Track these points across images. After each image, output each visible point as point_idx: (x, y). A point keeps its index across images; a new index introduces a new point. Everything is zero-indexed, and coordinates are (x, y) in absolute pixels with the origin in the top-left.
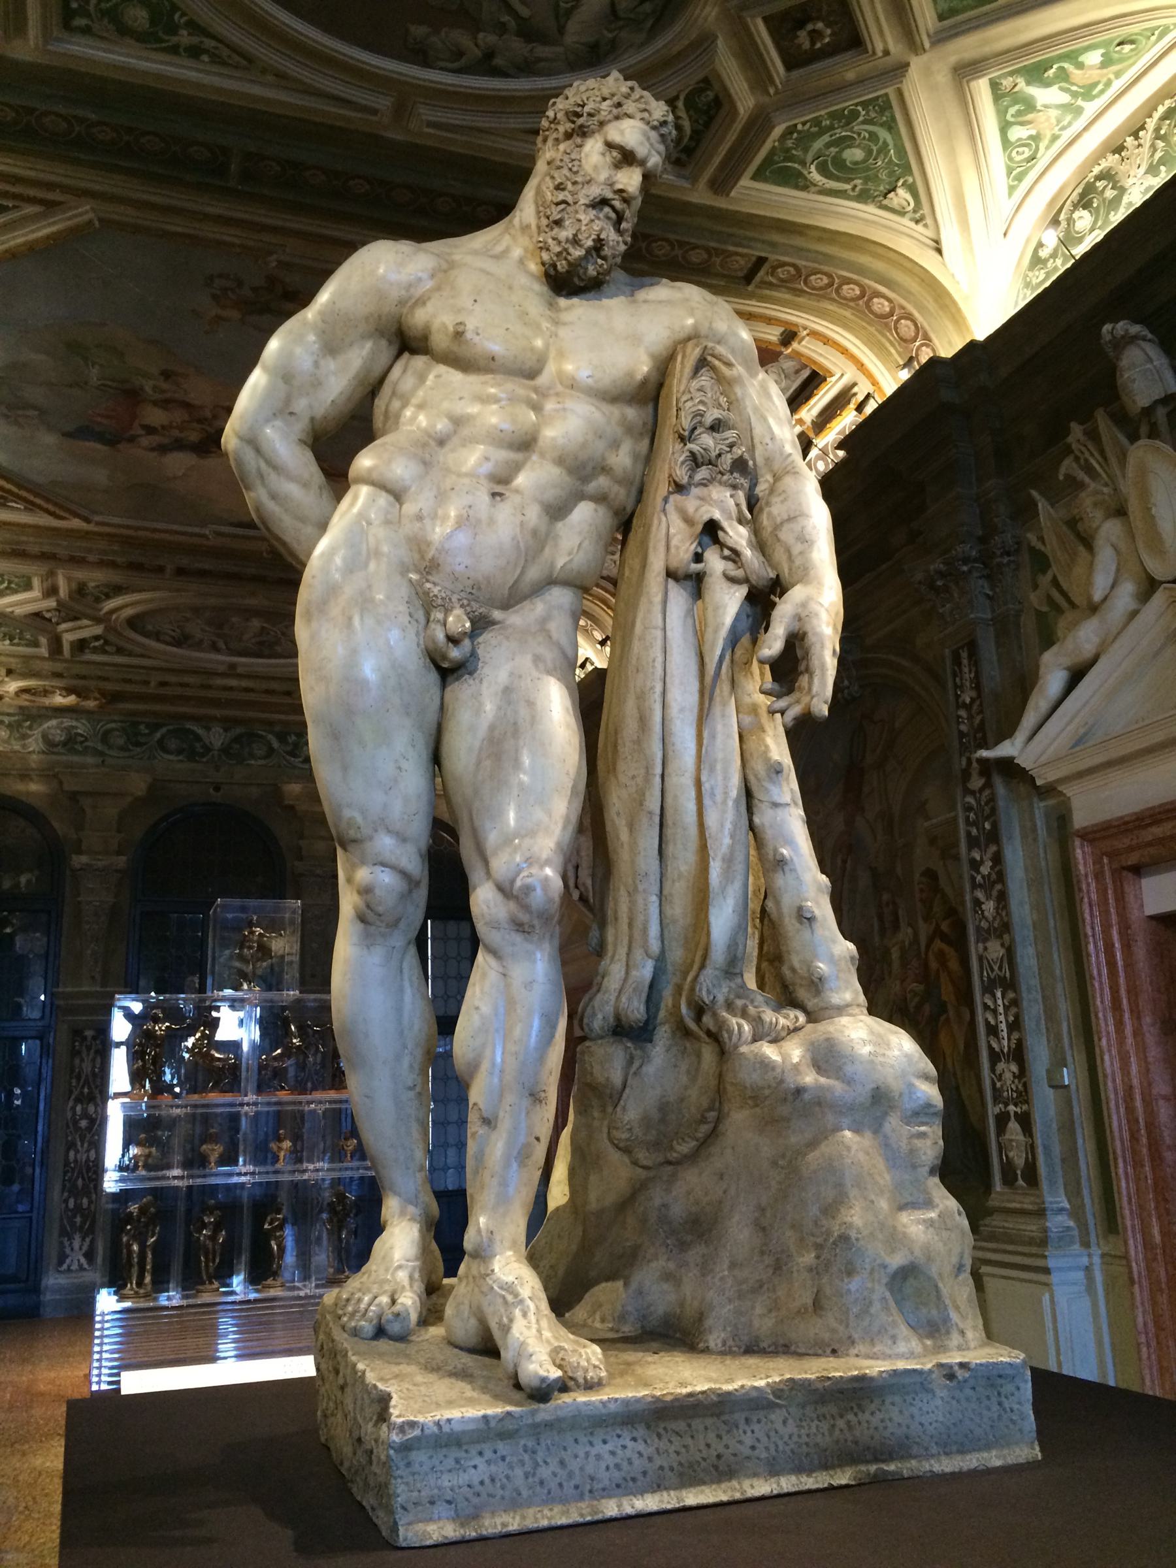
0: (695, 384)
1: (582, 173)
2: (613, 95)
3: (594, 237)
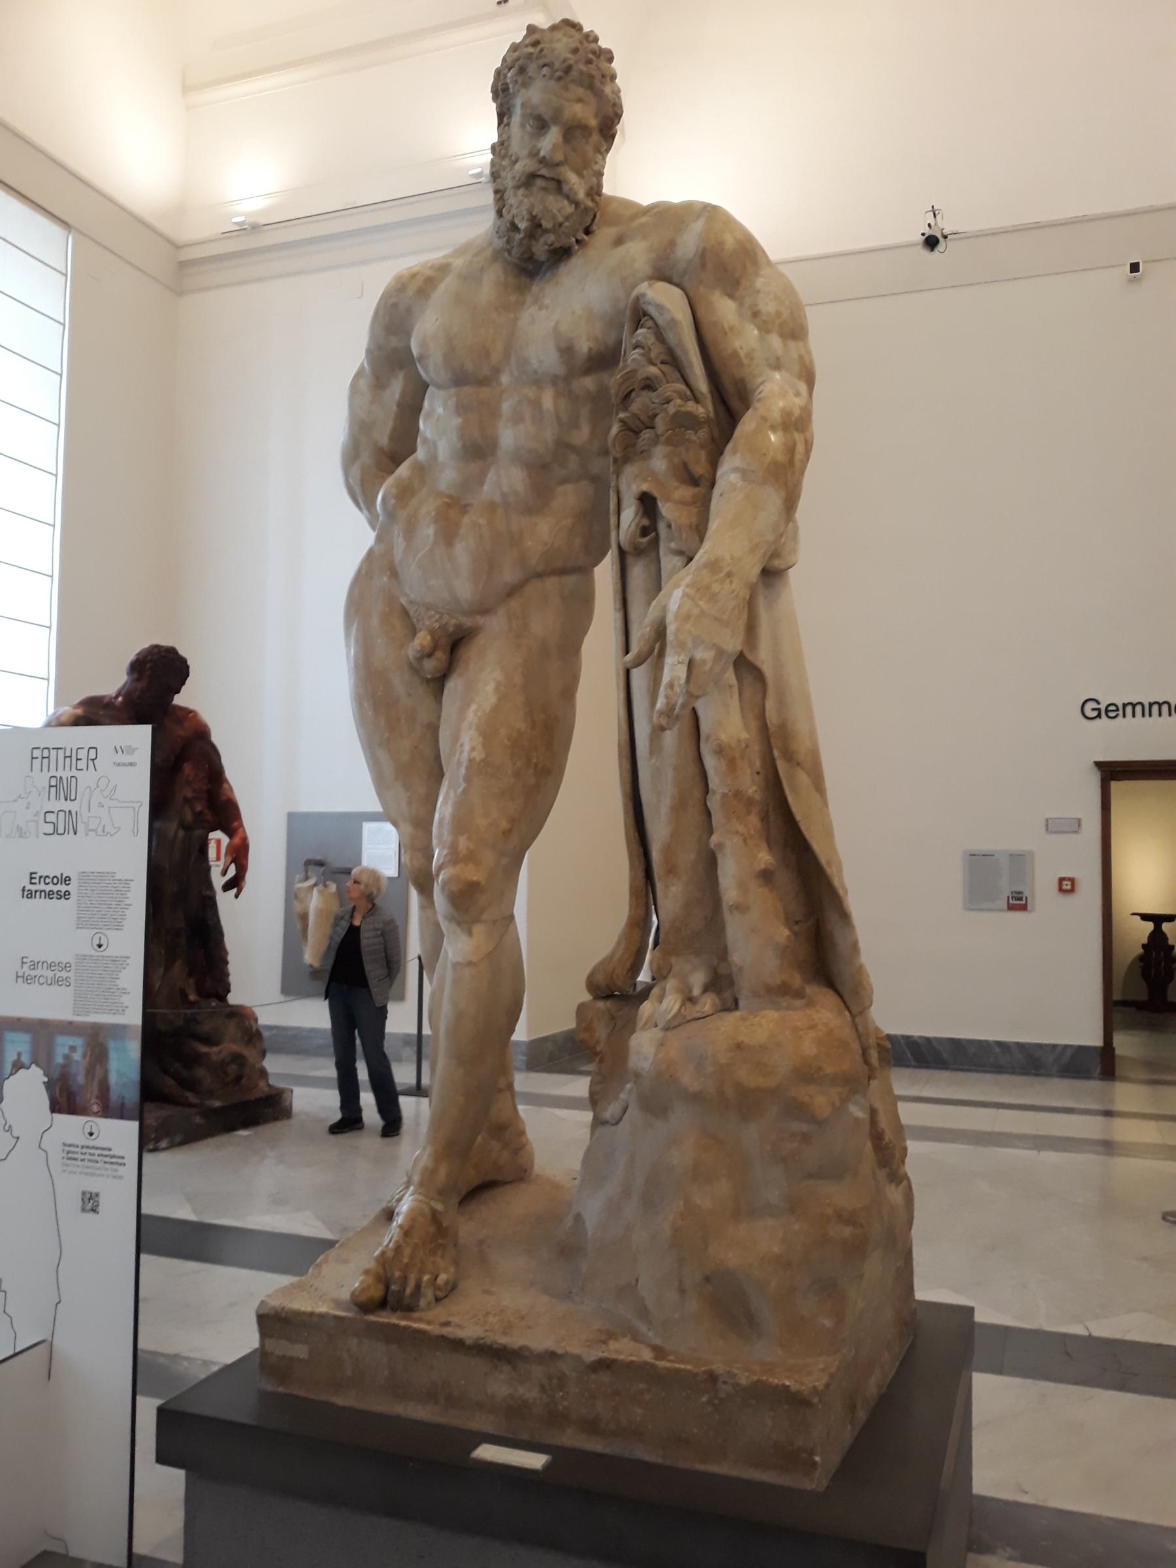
1: (510, 154)
3: (526, 217)
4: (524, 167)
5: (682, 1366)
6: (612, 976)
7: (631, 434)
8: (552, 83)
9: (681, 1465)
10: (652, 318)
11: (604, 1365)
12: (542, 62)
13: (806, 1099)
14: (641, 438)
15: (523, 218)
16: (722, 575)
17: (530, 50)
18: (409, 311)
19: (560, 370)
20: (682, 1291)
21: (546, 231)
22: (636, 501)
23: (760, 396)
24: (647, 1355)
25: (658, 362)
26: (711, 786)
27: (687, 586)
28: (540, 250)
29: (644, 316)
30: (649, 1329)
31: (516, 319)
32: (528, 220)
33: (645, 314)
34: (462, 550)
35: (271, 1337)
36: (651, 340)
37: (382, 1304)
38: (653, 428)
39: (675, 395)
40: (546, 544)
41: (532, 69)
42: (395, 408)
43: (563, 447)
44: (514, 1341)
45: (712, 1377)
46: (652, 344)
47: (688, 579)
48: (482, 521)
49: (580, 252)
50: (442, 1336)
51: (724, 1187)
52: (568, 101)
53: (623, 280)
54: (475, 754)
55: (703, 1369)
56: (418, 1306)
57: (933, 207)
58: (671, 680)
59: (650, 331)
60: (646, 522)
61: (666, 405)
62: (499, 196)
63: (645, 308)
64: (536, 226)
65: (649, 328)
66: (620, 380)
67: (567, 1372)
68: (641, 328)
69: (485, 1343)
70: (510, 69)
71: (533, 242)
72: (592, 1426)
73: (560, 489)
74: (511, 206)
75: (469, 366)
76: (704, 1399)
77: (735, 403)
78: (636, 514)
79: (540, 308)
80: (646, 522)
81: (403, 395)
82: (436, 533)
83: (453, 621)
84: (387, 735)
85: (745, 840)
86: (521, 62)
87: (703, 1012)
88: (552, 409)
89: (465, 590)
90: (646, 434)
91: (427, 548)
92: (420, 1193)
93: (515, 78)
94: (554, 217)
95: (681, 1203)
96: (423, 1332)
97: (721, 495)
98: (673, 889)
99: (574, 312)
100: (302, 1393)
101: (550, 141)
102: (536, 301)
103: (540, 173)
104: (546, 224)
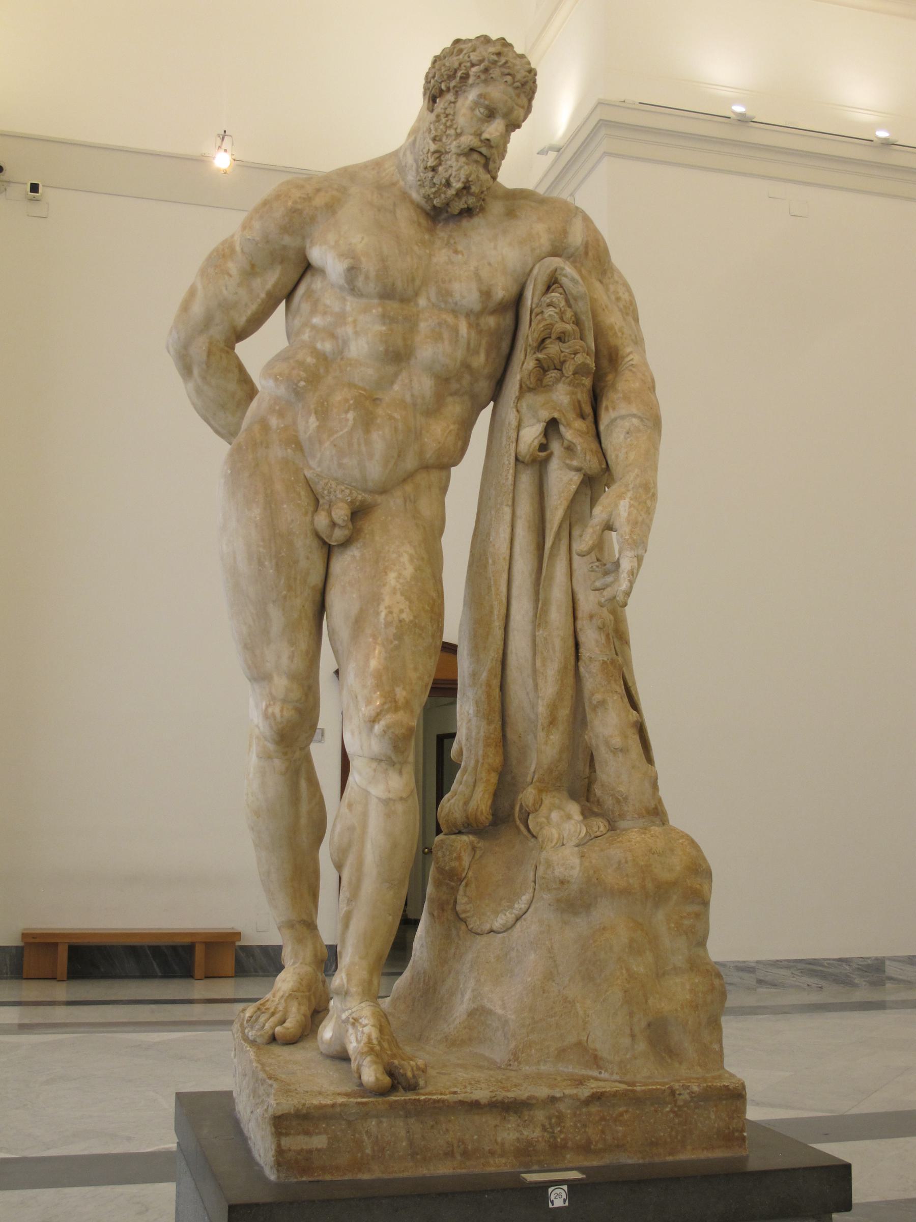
0: (547, 299)
1: (455, 126)
2: (481, 61)
4: (471, 141)
5: (654, 1087)
6: (476, 814)
7: (542, 371)
8: (510, 90)
9: (657, 1160)
10: (562, 287)
11: (597, 1097)
12: (506, 71)
13: (698, 886)
14: (548, 376)
15: (460, 179)
16: (651, 494)
17: (495, 58)
18: (313, 219)
19: (477, 307)
20: (633, 1036)
21: (473, 194)
22: (545, 424)
23: (631, 362)
24: (623, 1086)
25: (571, 322)
26: (584, 653)
27: (631, 499)
28: (460, 205)
29: (553, 284)
30: (600, 1073)
31: (430, 256)
32: (463, 182)
33: (556, 281)
34: (379, 440)
35: (287, 1134)
36: (563, 303)
37: (393, 1088)
38: (561, 370)
39: (581, 350)
40: (439, 443)
41: (496, 72)
42: (263, 295)
43: (466, 366)
44: (522, 1092)
45: (673, 1092)
46: (563, 307)
47: (629, 494)
48: (397, 416)
49: (481, 215)
50: (460, 1101)
51: (649, 957)
52: (517, 105)
53: (533, 250)
54: (404, 616)
55: (667, 1086)
56: (419, 1085)
57: (225, 132)
58: (631, 569)
59: (562, 296)
60: (544, 441)
61: (573, 356)
62: (437, 155)
63: (559, 277)
64: (466, 188)
65: (561, 294)
66: (542, 329)
67: (563, 1111)
68: (552, 292)
69: (497, 1100)
70: (473, 65)
71: (456, 199)
72: (586, 1148)
73: (449, 399)
74: (452, 167)
75: (399, 285)
76: (668, 1109)
77: (605, 363)
78: (540, 434)
79: (456, 252)
80: (544, 441)
81: (275, 286)
82: (354, 419)
83: (360, 497)
84: (285, 592)
85: (621, 698)
86: (486, 63)
87: (602, 832)
88: (465, 335)
89: (375, 471)
90: (553, 374)
91: (346, 430)
92: (366, 1001)
93: (478, 74)
94: (481, 186)
95: (624, 971)
96: (443, 1101)
97: (628, 433)
98: (552, 737)
99: (490, 264)
100: (328, 1177)
101: (494, 129)
102: (448, 244)
103: (480, 150)
104: (474, 189)
